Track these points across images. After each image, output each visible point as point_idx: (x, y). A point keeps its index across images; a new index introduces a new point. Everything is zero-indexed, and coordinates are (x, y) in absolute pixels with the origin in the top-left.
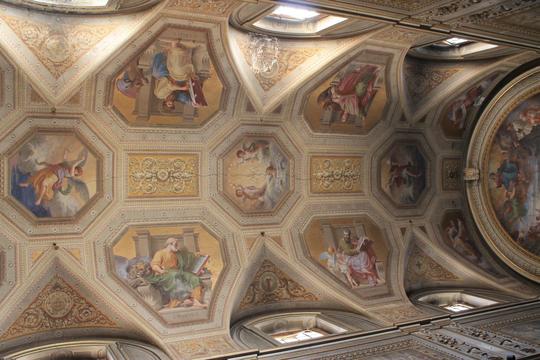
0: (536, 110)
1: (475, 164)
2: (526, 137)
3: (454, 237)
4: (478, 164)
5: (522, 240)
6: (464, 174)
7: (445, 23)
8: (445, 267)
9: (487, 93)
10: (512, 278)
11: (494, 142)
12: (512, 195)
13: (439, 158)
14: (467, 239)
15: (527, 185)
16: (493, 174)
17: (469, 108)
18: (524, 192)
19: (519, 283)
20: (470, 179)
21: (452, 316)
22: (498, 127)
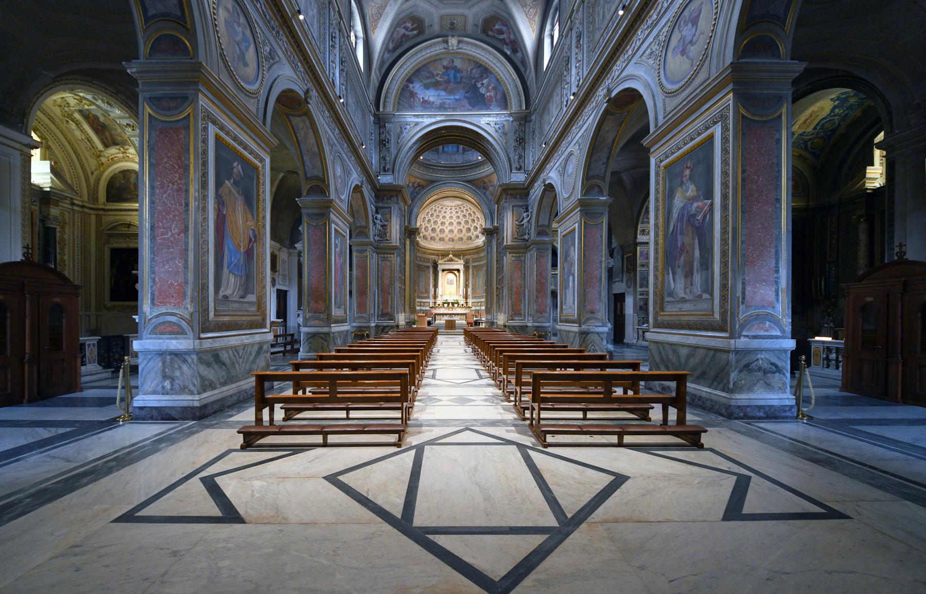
1: (461, 45)
2: (478, 89)
5: (407, 87)
6: (453, 36)
9: (513, 57)
11: (476, 62)
12: (438, 78)
13: (466, 12)
15: (445, 90)
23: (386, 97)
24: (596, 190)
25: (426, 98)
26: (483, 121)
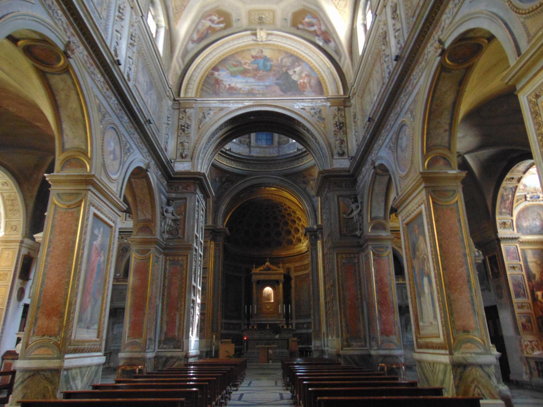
0: (309, 83)
1: (270, 37)
2: (290, 76)
3: (210, 20)
4: (270, 40)
5: (212, 74)
6: (261, 29)
7: (384, 10)
8: (184, 13)
10: (183, 67)
11: (286, 53)
12: (246, 67)
13: (274, 7)
14: (210, 32)
15: (254, 77)
16: (262, 52)
17: (315, 33)
18: (249, 75)
19: (179, 72)
20: (258, 34)
21: (143, 17)
22: (298, 55)
23: (188, 84)
24: (442, 162)
25: (233, 85)
26: (297, 106)
